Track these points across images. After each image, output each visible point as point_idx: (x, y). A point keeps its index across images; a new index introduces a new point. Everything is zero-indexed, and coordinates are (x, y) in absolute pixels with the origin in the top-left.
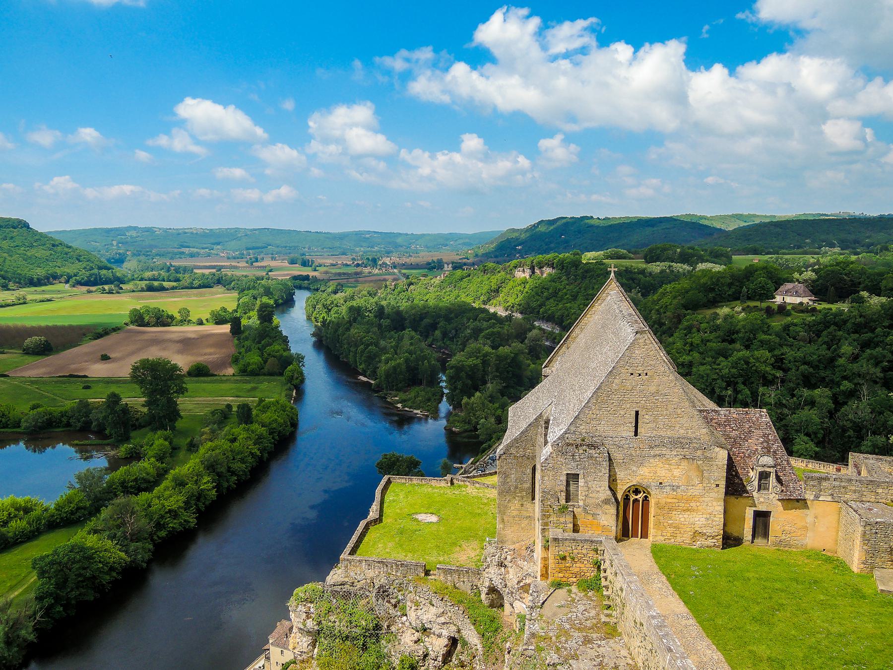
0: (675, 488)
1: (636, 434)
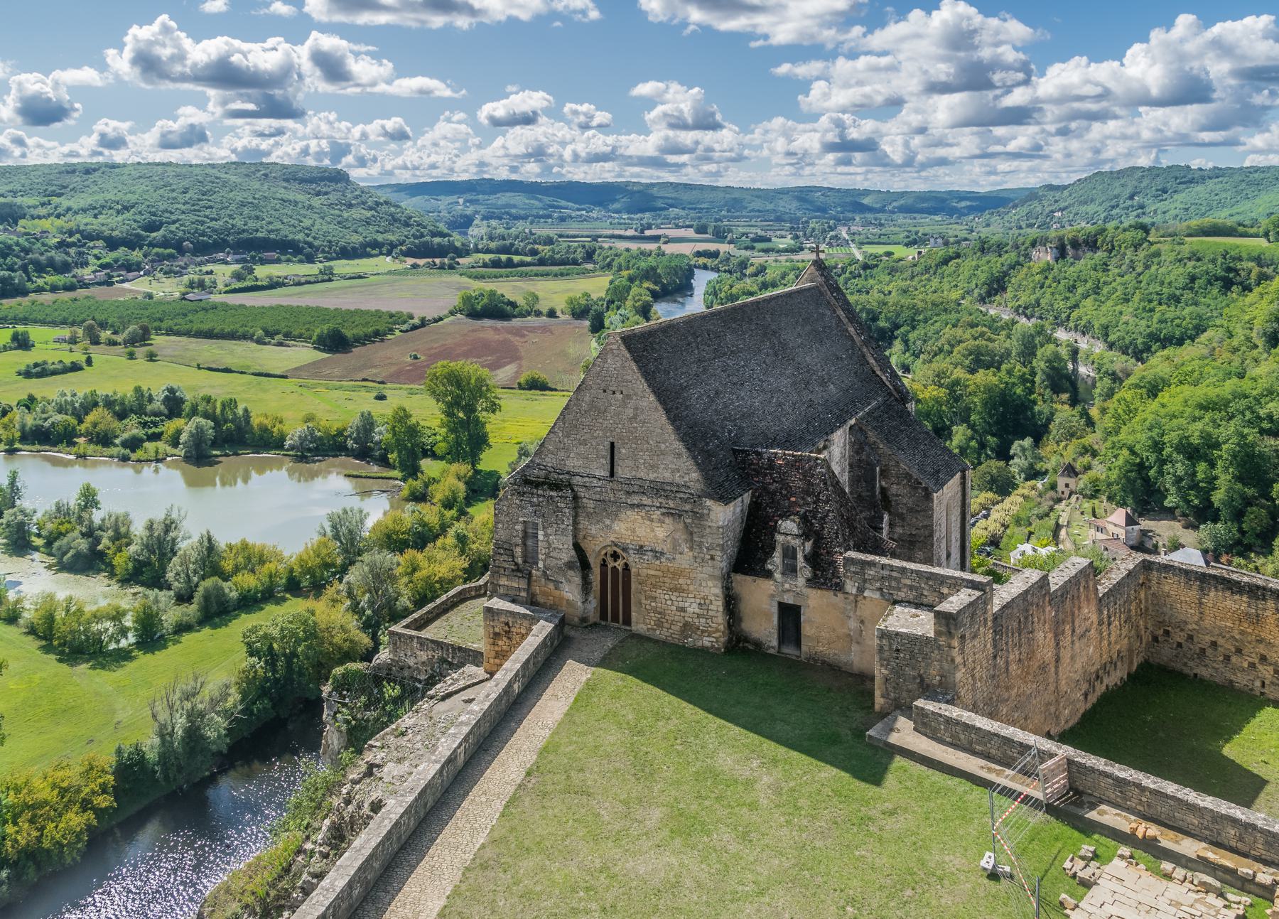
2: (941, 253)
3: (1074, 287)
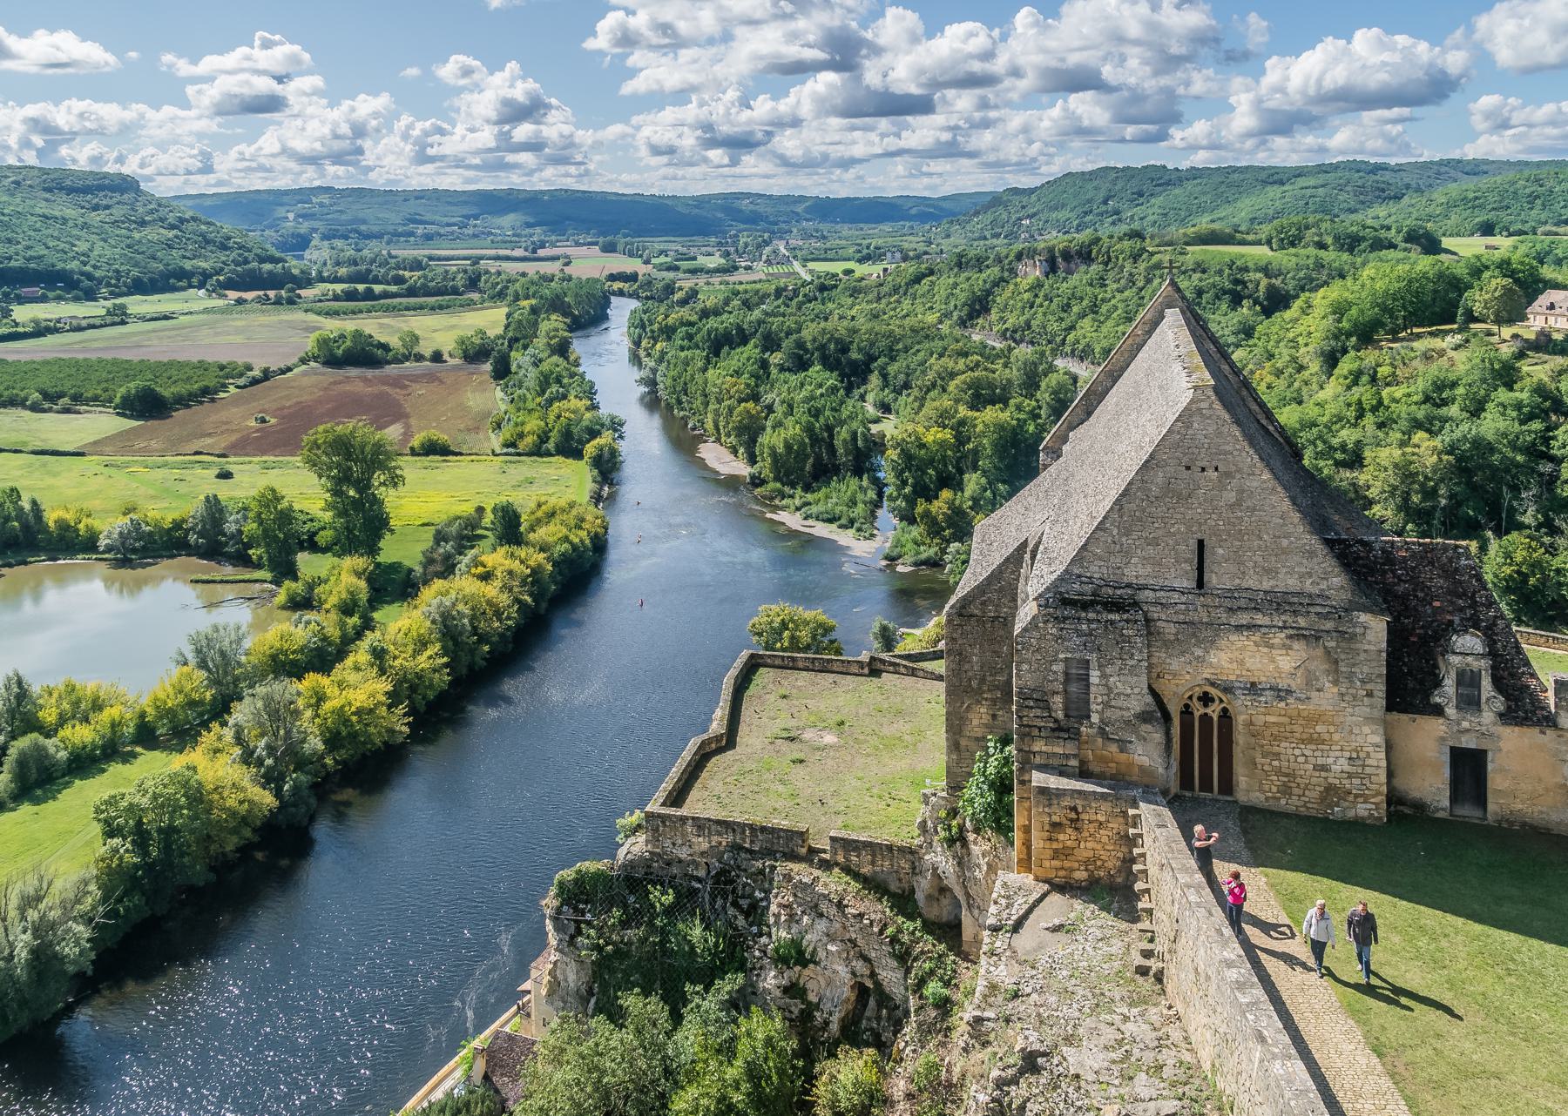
0: (1282, 693)
1: (1200, 583)
2: (910, 269)
3: (1068, 305)
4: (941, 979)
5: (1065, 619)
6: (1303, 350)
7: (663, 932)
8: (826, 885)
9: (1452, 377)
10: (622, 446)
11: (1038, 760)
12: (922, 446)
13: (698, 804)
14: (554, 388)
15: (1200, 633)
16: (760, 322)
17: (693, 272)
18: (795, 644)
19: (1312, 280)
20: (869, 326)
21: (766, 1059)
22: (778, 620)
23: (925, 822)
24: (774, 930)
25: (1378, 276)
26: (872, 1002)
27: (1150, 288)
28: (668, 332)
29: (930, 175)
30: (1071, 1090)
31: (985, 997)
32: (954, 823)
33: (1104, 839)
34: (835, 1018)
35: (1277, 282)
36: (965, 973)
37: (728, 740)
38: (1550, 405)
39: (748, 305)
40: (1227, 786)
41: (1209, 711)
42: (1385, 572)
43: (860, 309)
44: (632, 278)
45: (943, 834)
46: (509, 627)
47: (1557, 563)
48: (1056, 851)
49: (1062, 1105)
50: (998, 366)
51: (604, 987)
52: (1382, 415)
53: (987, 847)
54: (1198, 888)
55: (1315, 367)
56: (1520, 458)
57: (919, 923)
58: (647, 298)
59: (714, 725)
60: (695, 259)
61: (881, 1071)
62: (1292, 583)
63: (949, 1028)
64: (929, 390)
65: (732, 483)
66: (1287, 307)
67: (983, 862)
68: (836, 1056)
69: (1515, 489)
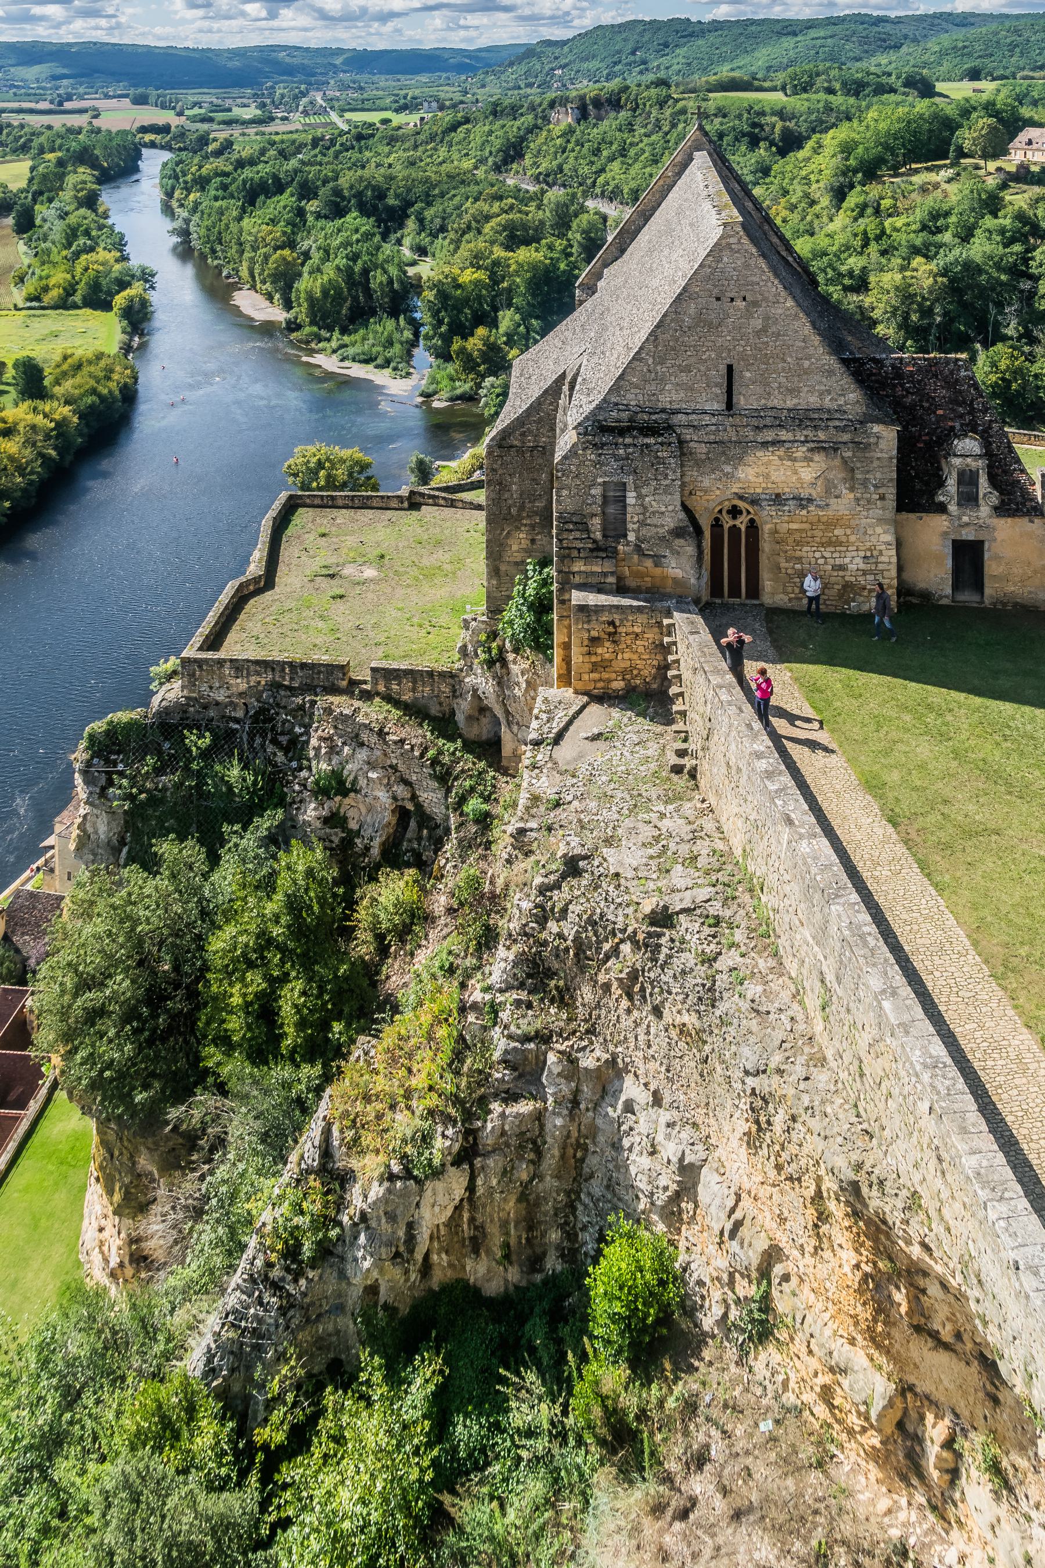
0: (803, 502)
2: (447, 117)
3: (599, 150)
4: (481, 795)
5: (603, 445)
6: (814, 186)
7: (200, 775)
8: (367, 714)
9: (945, 207)
10: (153, 297)
11: (577, 580)
12: (459, 286)
13: (238, 646)
14: (82, 241)
15: (729, 451)
16: (296, 171)
17: (229, 123)
18: (331, 483)
19: (822, 122)
20: (406, 173)
21: (307, 890)
22: (314, 460)
23: (465, 646)
24: (314, 763)
25: (882, 118)
26: (413, 824)
27: (674, 134)
28: (202, 183)
29: (466, 28)
30: (611, 889)
31: (527, 808)
32: (494, 645)
33: (641, 649)
34: (376, 843)
35: (791, 125)
36: (505, 788)
37: (267, 581)
38: (1029, 230)
39: (284, 155)
40: (754, 590)
41: (737, 523)
42: (895, 386)
43: (397, 157)
44: (165, 129)
45: (483, 656)
46: (31, 483)
47: (1035, 369)
48: (594, 664)
49: (602, 904)
50: (532, 207)
51: (137, 835)
52: (885, 243)
53: (525, 665)
54: (729, 688)
55: (825, 201)
56: (1003, 277)
57: (459, 743)
58: (180, 149)
59: (252, 567)
60: (230, 110)
61: (423, 889)
62: (813, 401)
63: (490, 843)
64: (464, 233)
65: (267, 329)
66: (800, 147)
67: (522, 680)
68: (377, 880)
69: (1000, 305)
